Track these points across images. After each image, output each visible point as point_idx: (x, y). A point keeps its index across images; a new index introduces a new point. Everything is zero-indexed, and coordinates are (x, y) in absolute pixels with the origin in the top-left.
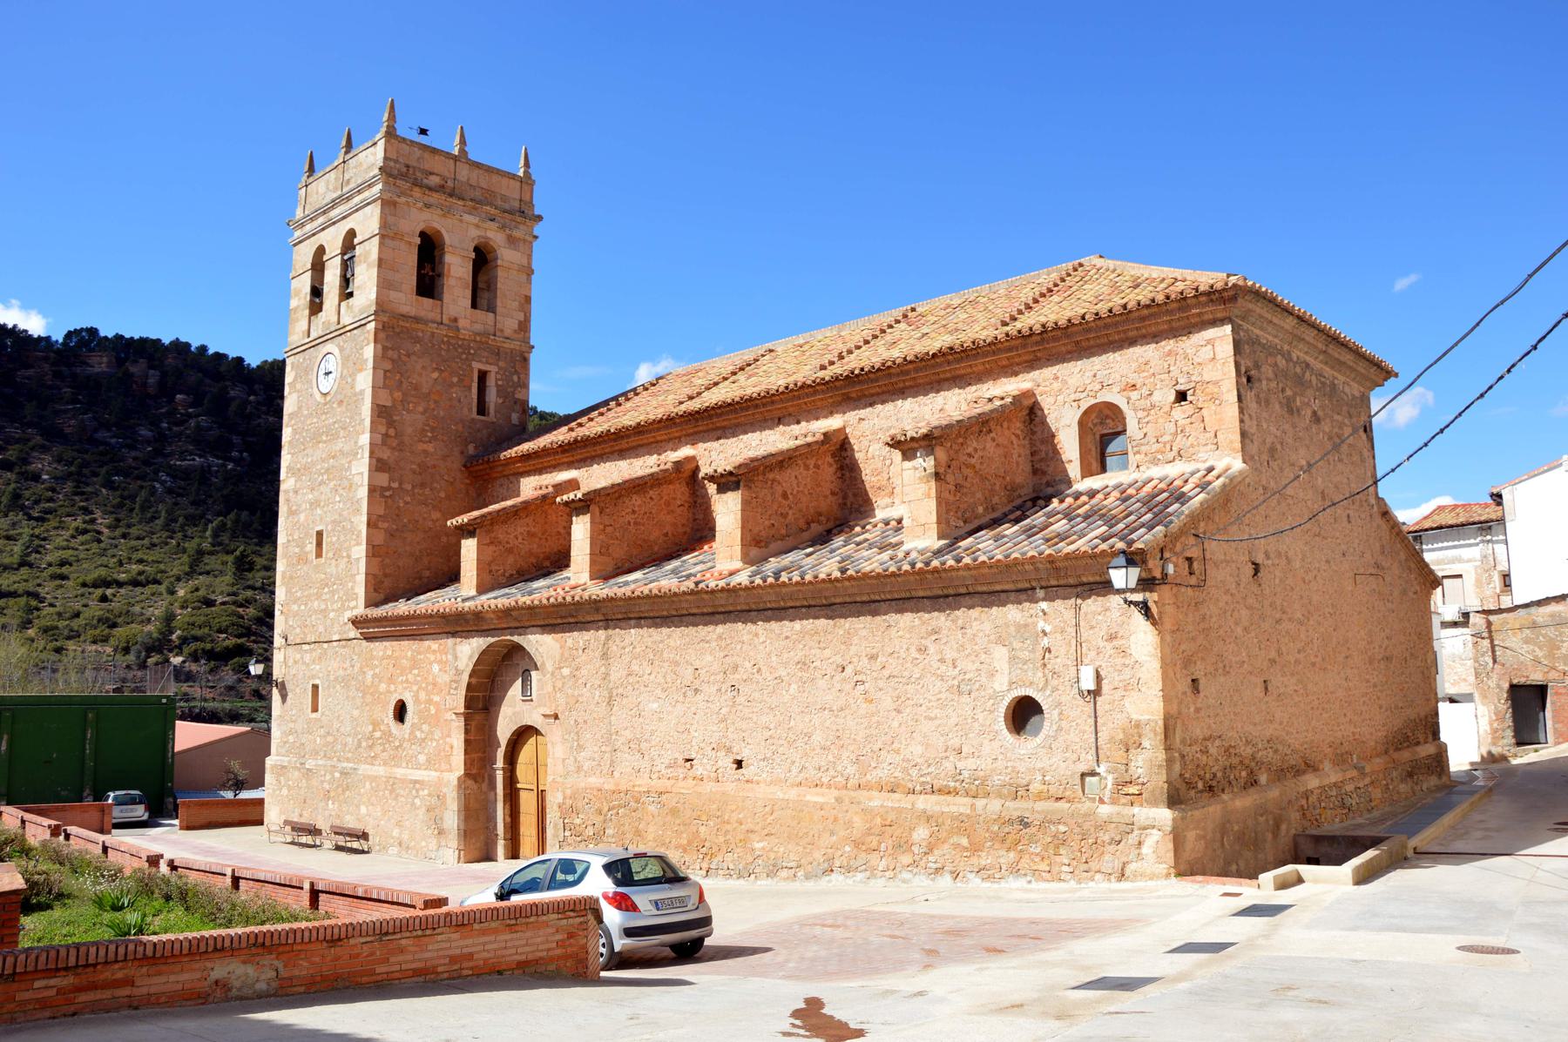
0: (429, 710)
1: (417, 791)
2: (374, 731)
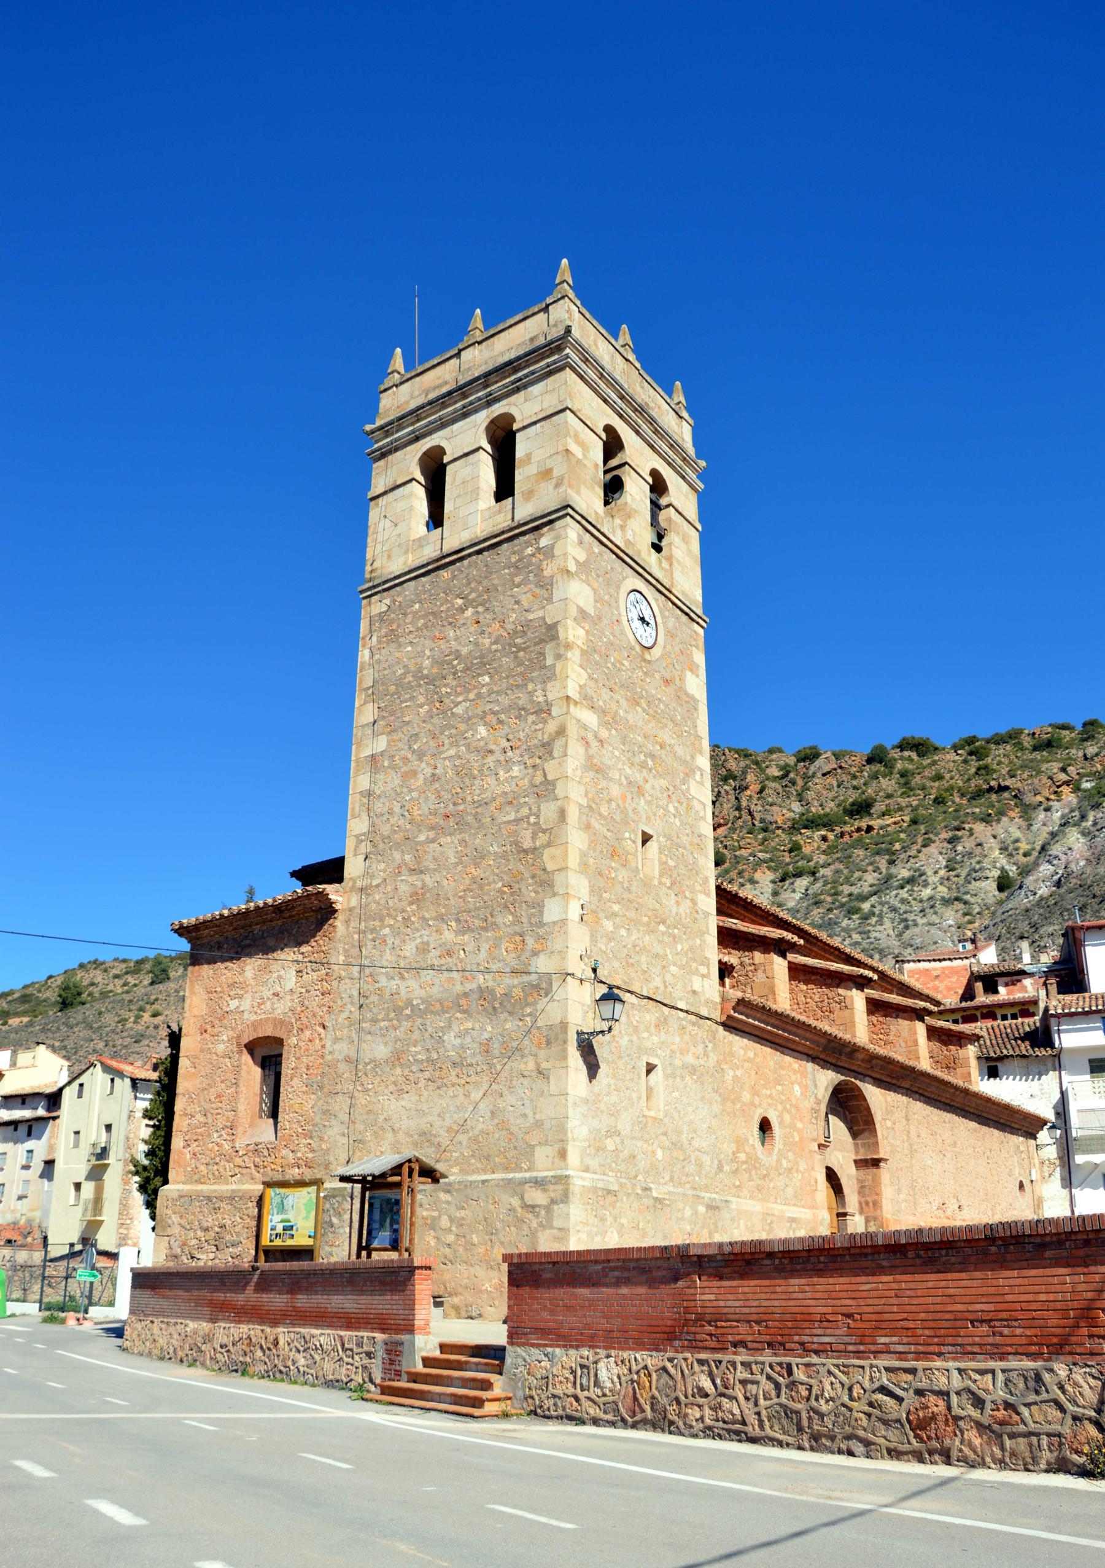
0: (793, 1137)
2: (738, 1151)
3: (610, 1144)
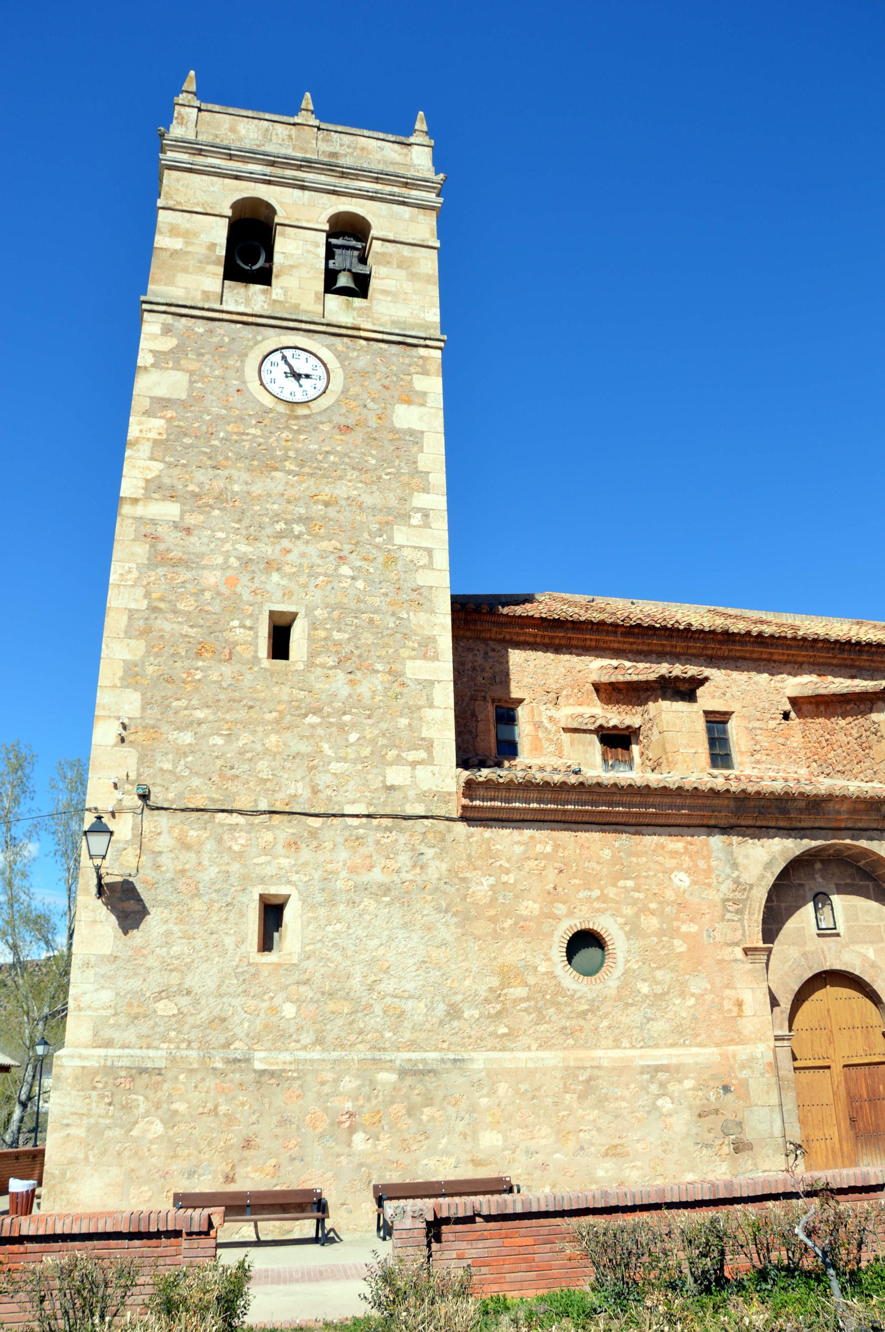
1: (662, 1085)
3: (164, 1008)
